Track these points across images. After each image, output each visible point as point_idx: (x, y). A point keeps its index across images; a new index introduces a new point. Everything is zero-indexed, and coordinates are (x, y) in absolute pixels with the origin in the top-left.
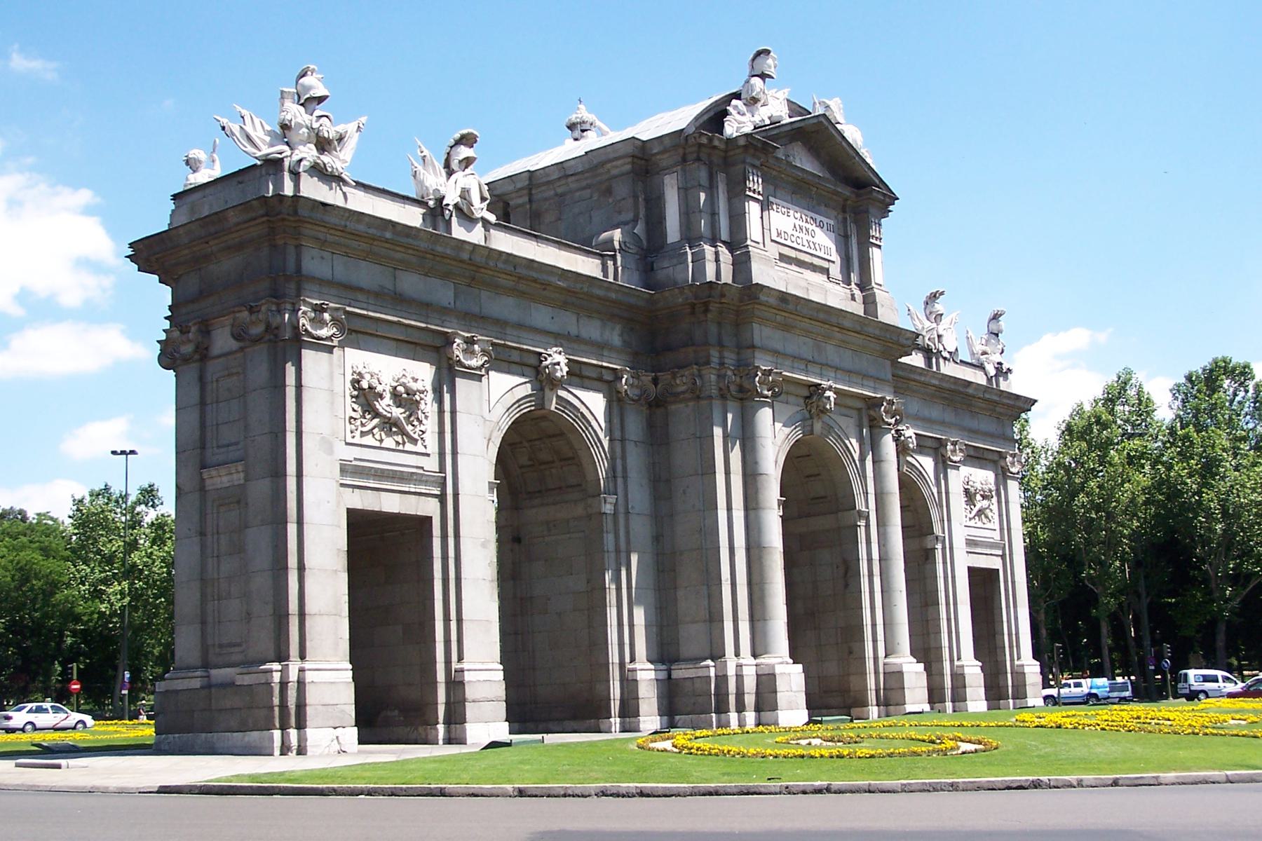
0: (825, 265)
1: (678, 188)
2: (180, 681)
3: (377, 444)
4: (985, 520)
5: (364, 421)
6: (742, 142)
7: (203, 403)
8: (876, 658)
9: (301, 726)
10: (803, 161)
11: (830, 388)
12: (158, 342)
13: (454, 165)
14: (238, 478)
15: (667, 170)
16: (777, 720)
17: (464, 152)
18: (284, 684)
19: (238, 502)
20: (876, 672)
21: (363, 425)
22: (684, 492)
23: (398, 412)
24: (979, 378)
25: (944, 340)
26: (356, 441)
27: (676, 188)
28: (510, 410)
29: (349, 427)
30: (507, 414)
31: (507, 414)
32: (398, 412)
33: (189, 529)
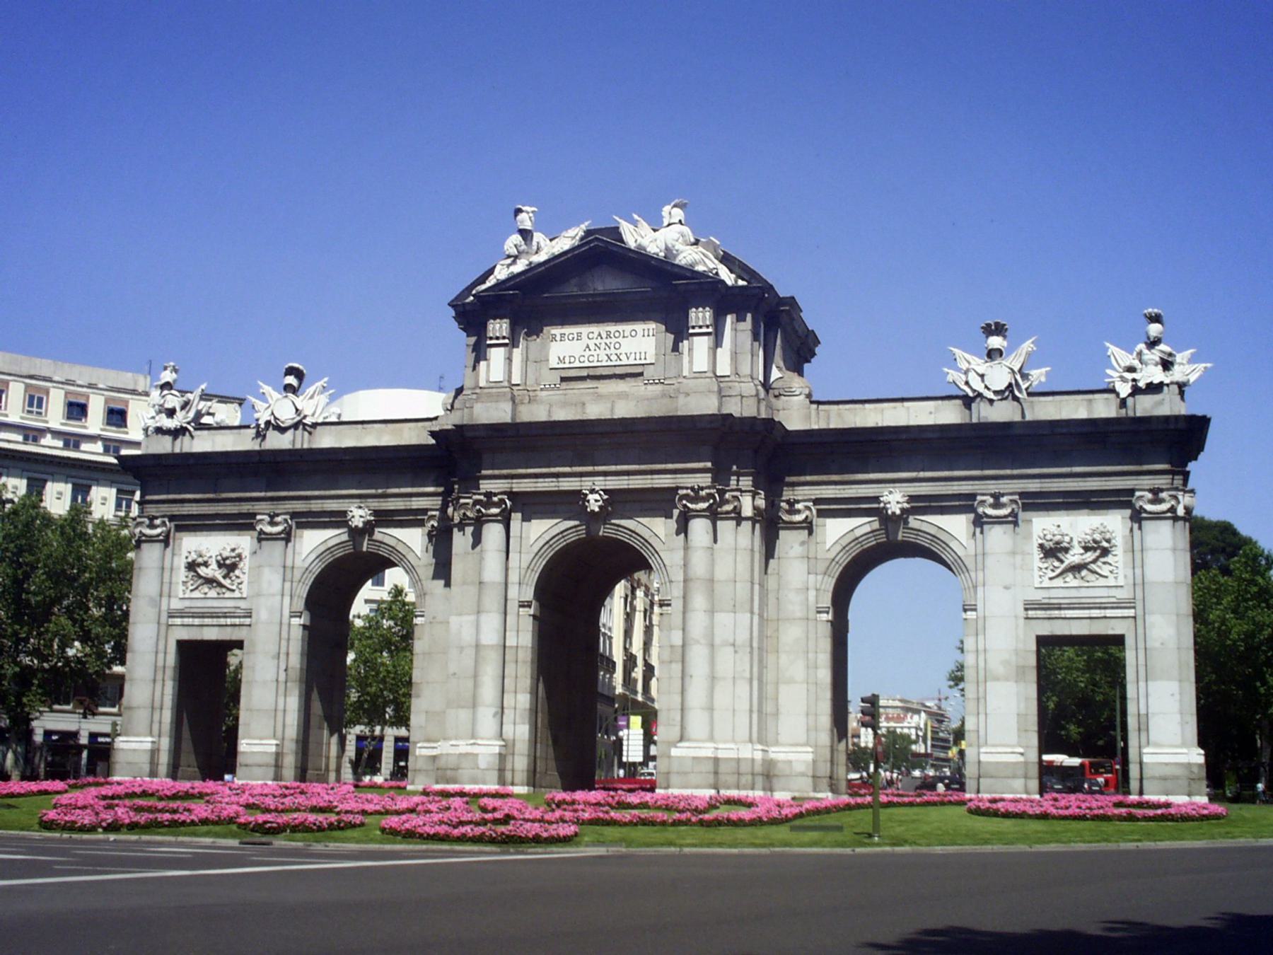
0: (639, 370)
3: (203, 596)
4: (1091, 577)
5: (192, 582)
10: (606, 283)
11: (592, 491)
17: (291, 380)
21: (192, 585)
23: (218, 574)
24: (1104, 409)
25: (985, 378)
26: (187, 596)
28: (321, 557)
29: (181, 588)
30: (317, 560)
31: (317, 560)
32: (218, 574)
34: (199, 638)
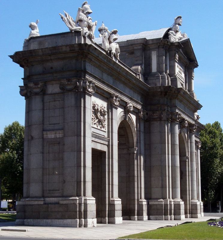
1: (157, 56)
2: (33, 202)
3: (96, 127)
5: (95, 120)
6: (176, 44)
7: (43, 109)
8: (189, 200)
9: (86, 217)
12: (19, 86)
13: (112, 40)
14: (59, 135)
15: (154, 49)
16: (180, 218)
18: (80, 204)
19: (59, 143)
20: (189, 204)
22: (155, 148)
27: (156, 55)
33: (37, 151)
34: (96, 148)
